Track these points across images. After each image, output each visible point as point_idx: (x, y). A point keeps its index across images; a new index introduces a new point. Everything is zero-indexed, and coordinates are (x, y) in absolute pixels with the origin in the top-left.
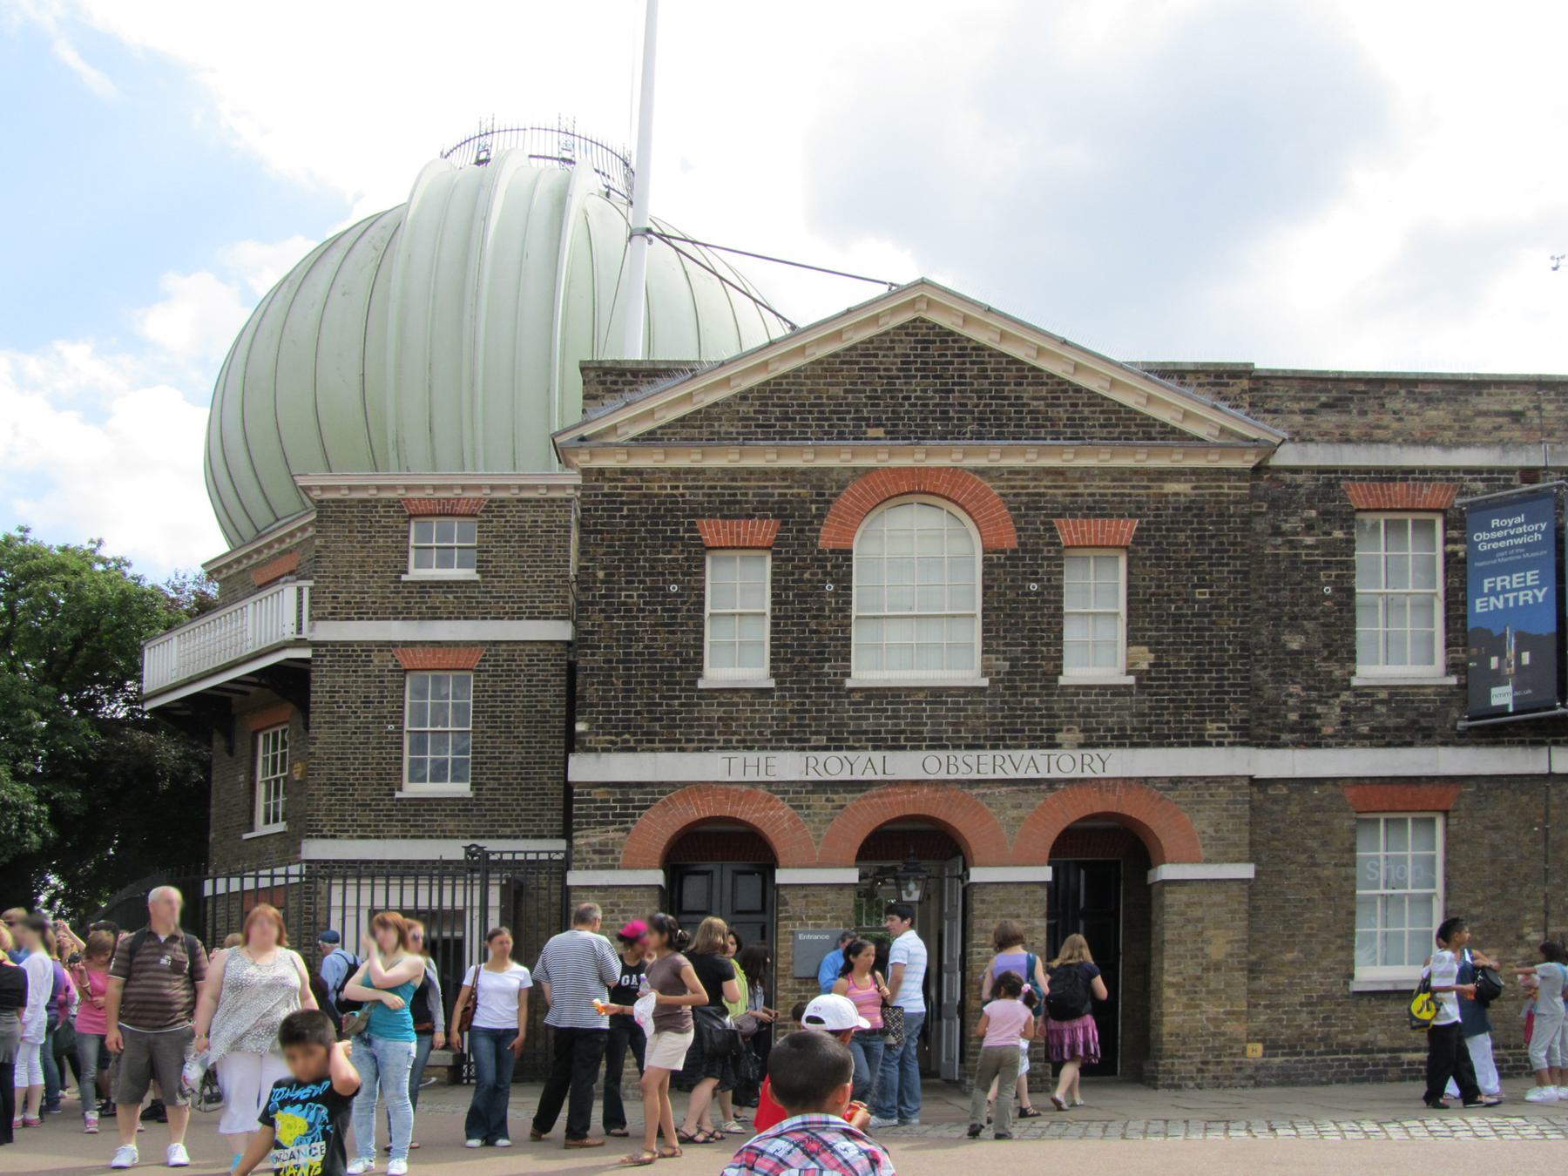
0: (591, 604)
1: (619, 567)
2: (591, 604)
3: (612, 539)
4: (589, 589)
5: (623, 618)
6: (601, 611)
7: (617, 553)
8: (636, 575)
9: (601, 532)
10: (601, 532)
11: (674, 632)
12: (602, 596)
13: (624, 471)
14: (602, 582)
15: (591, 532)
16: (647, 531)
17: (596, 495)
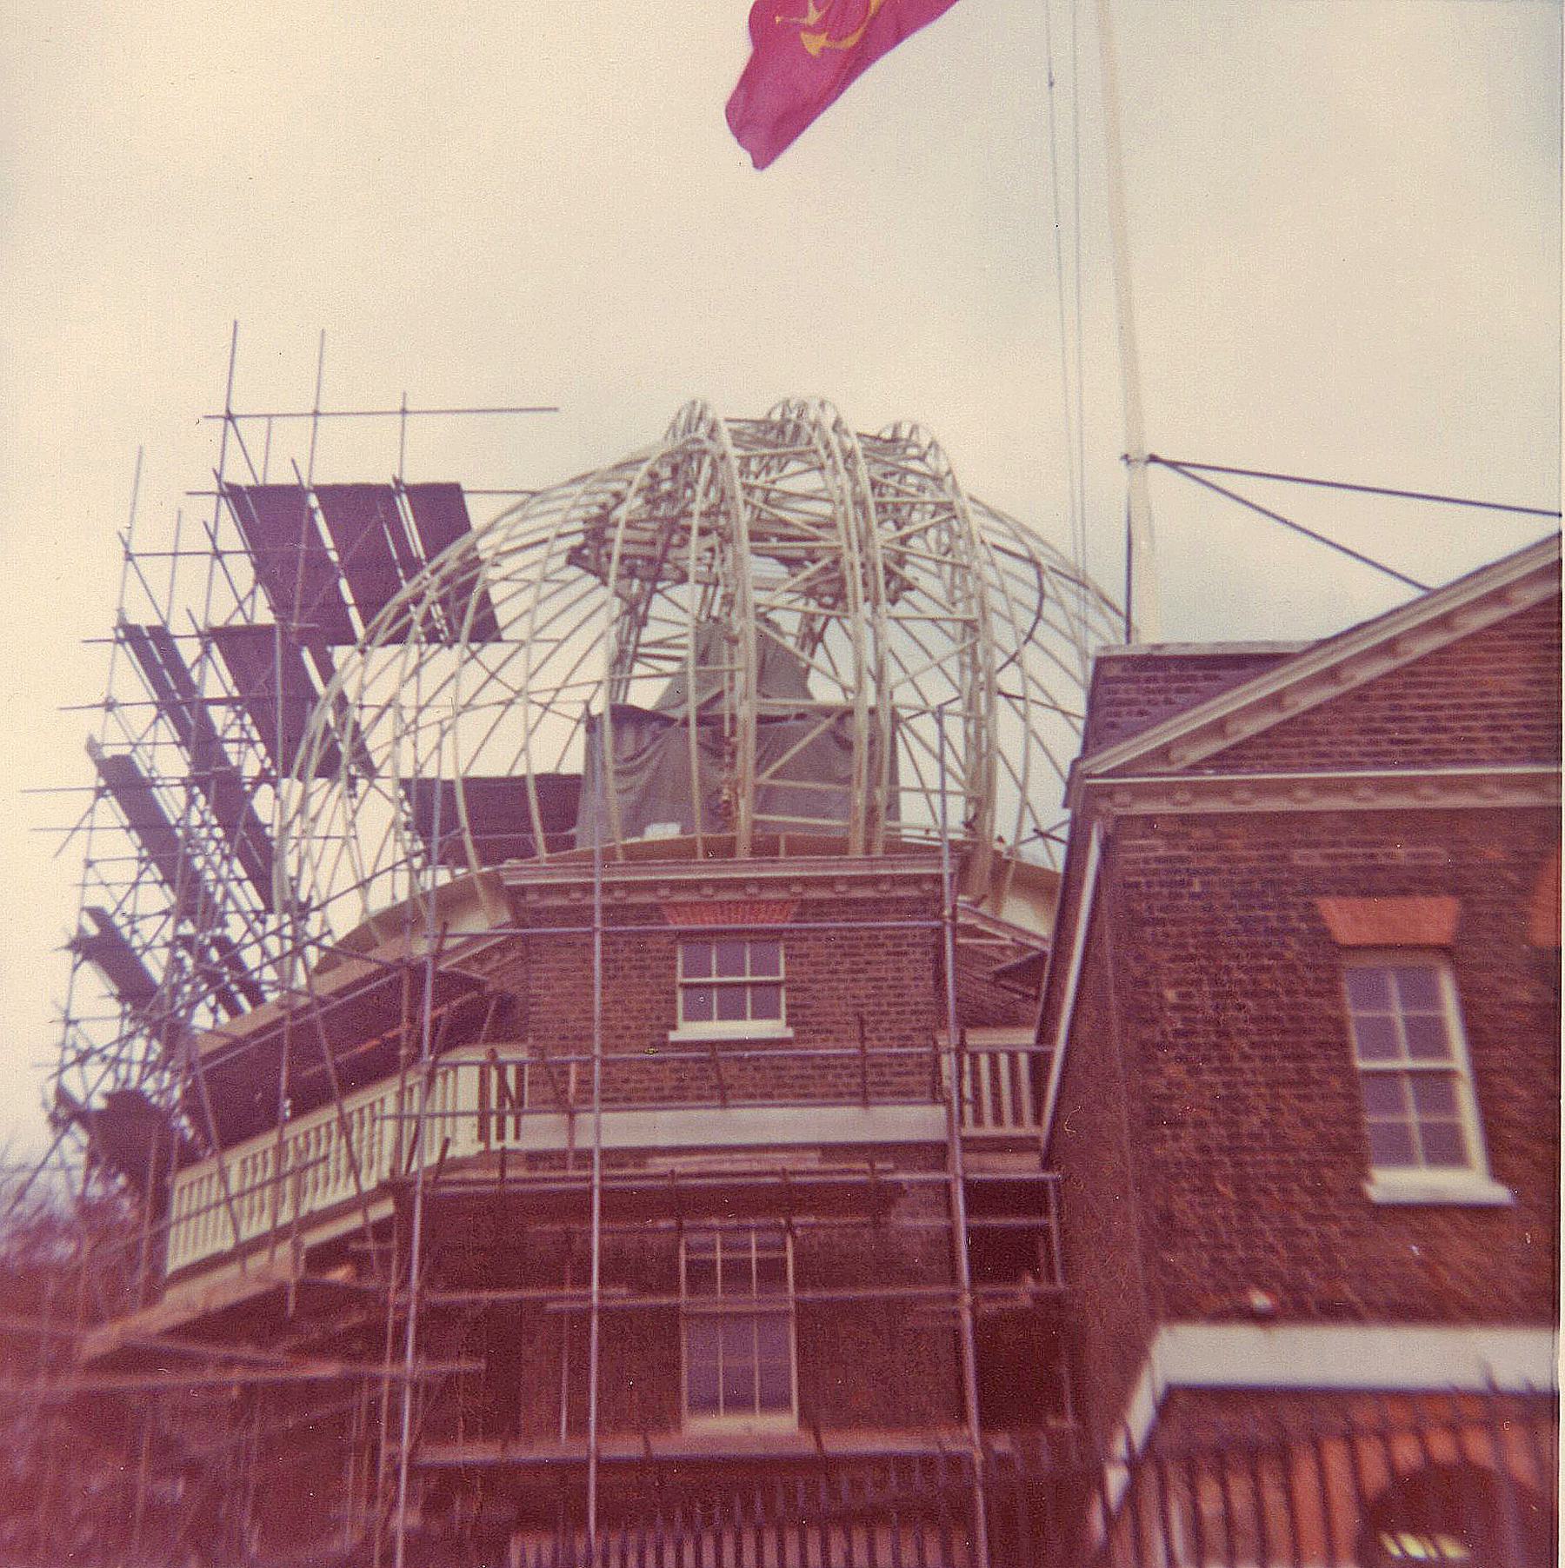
0: (1160, 1046)
1: (1198, 983)
2: (1160, 1046)
3: (1182, 934)
4: (1154, 1021)
5: (1217, 1071)
6: (1181, 1059)
7: (1192, 958)
8: (1230, 994)
9: (1162, 922)
10: (1162, 922)
11: (1307, 1098)
12: (1177, 1033)
13: (1185, 819)
14: (1175, 1008)
15: (1145, 923)
16: (1240, 920)
17: (1146, 861)
